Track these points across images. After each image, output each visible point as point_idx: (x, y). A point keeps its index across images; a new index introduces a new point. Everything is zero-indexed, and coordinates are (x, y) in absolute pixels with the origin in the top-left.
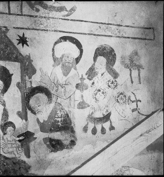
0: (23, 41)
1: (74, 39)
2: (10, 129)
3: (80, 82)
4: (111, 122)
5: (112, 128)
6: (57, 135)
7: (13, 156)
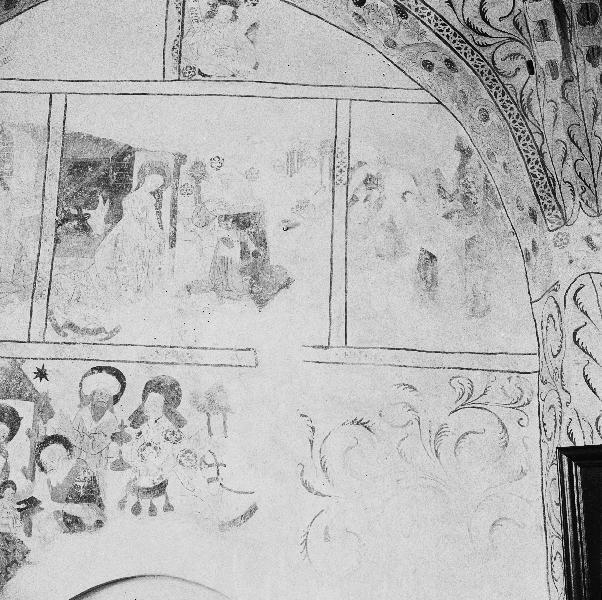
0: (41, 374)
1: (114, 369)
2: (9, 491)
3: (118, 430)
4: (167, 498)
5: (168, 508)
6: (75, 509)
7: (8, 531)
